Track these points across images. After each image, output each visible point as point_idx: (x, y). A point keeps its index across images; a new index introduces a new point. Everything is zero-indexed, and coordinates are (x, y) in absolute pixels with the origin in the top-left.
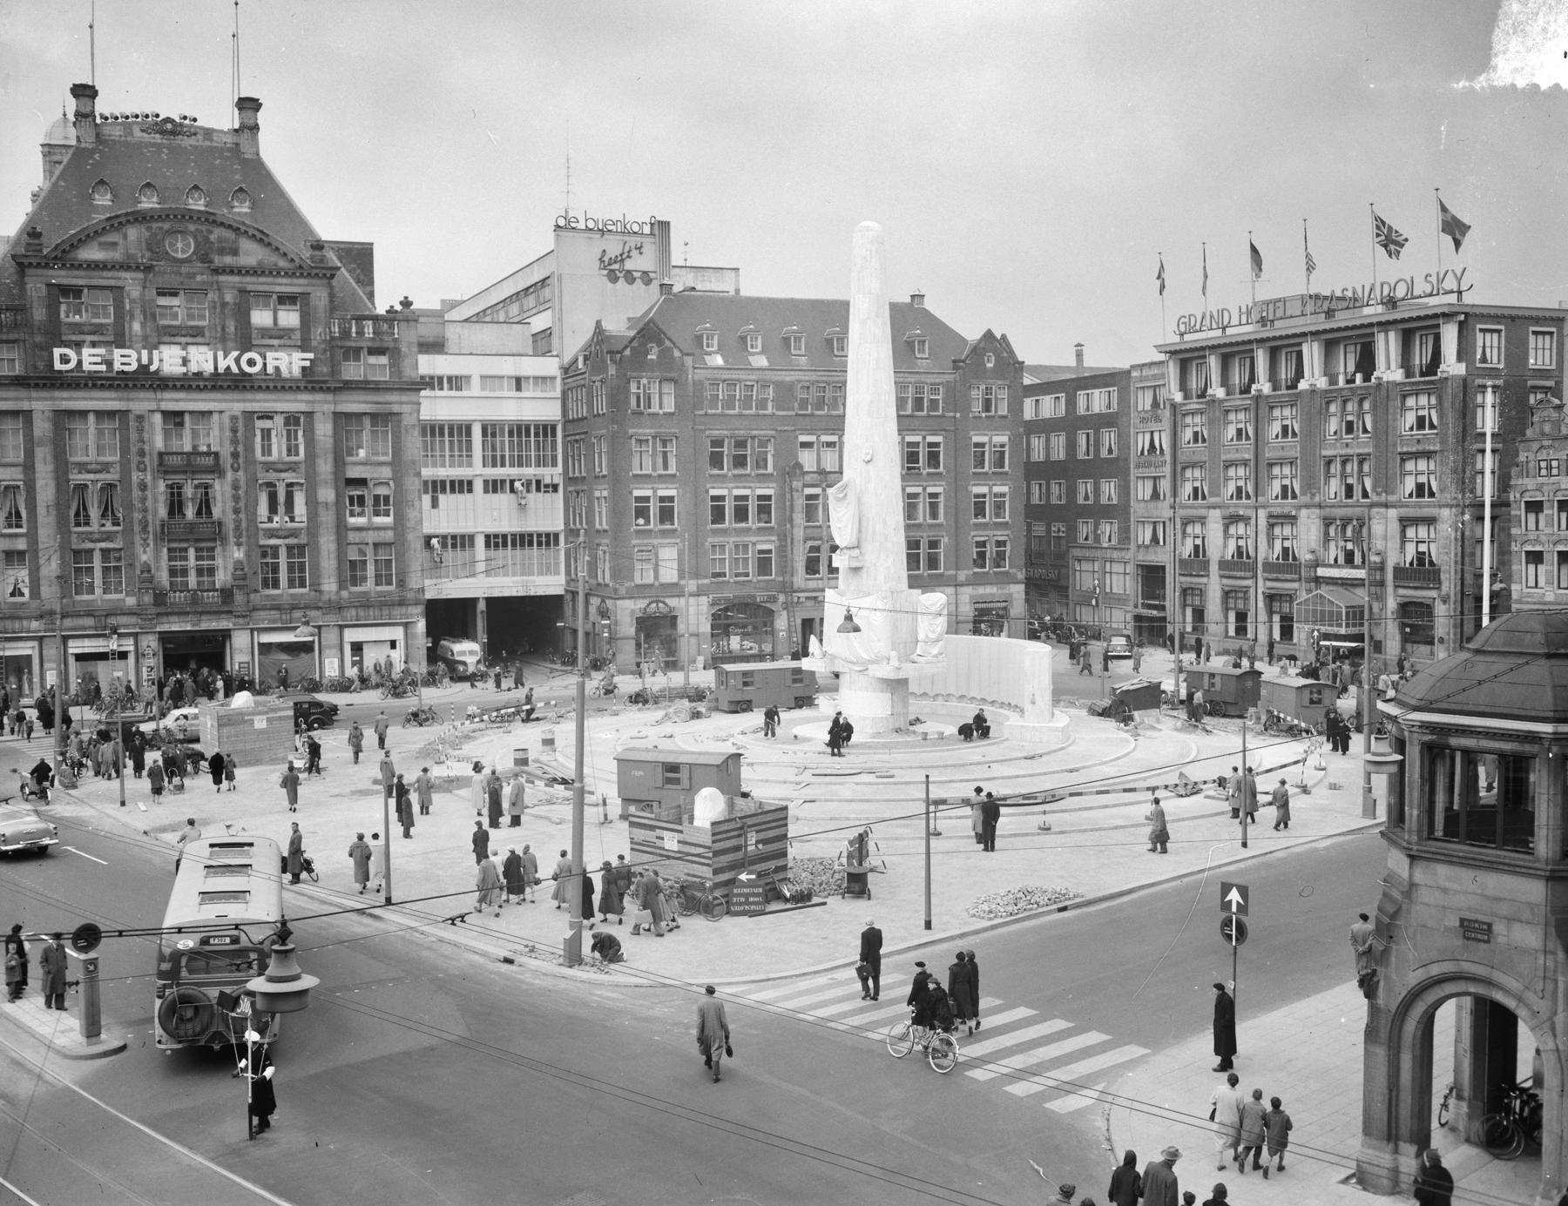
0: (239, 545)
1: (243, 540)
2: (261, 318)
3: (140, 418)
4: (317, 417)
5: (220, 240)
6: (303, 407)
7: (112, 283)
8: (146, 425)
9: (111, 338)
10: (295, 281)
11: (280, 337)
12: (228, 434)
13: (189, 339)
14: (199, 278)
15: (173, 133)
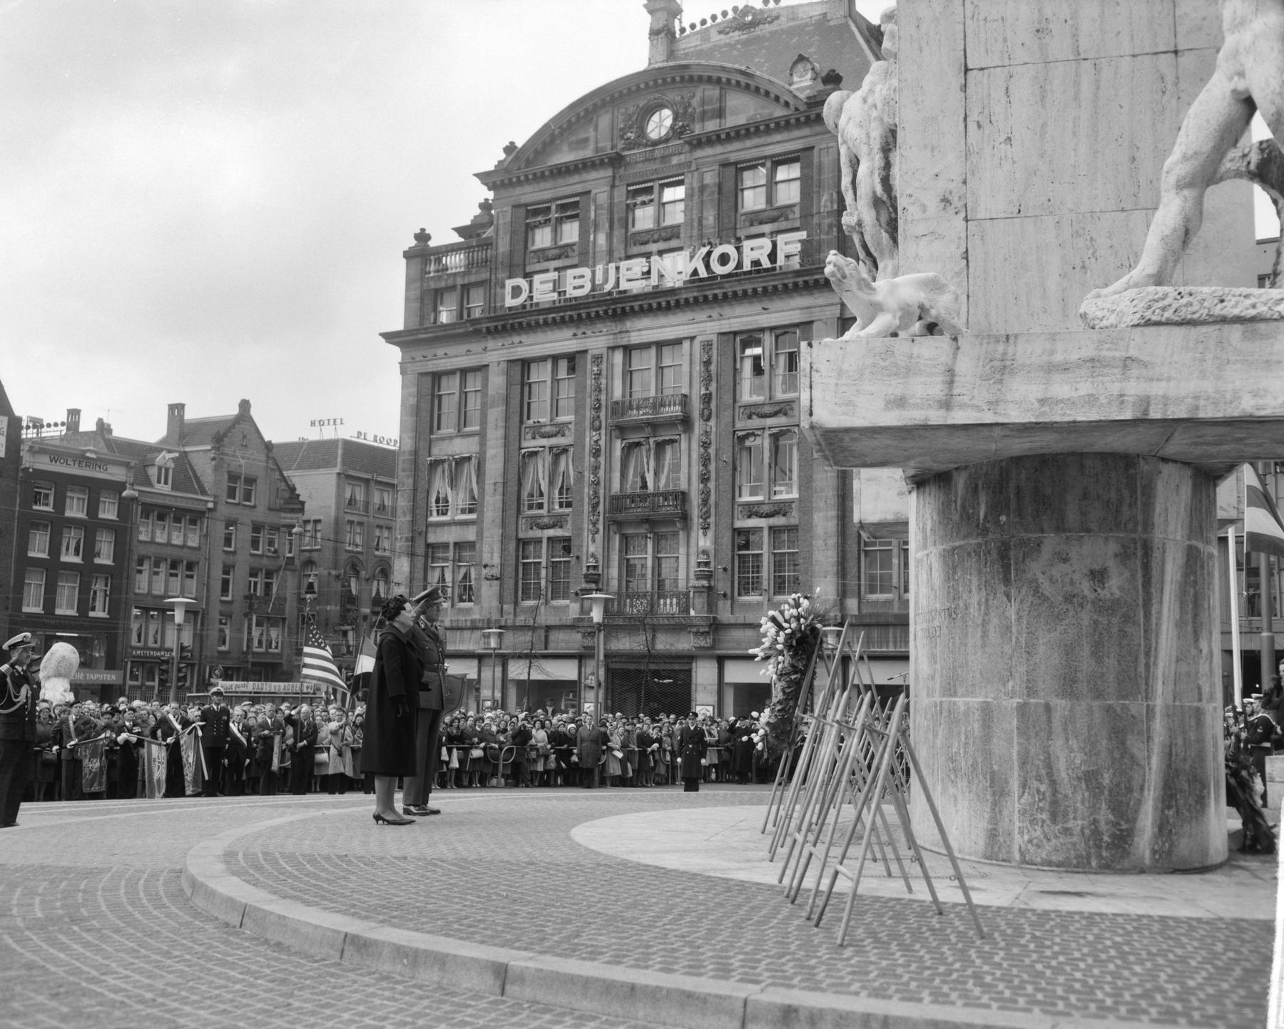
0: (705, 529)
1: (712, 520)
2: (752, 200)
3: (598, 359)
4: (815, 325)
5: (703, 102)
6: (796, 317)
7: (579, 188)
8: (604, 366)
9: (575, 261)
10: (797, 133)
11: (773, 220)
12: (698, 368)
13: (662, 245)
14: (675, 160)
15: (753, 24)
